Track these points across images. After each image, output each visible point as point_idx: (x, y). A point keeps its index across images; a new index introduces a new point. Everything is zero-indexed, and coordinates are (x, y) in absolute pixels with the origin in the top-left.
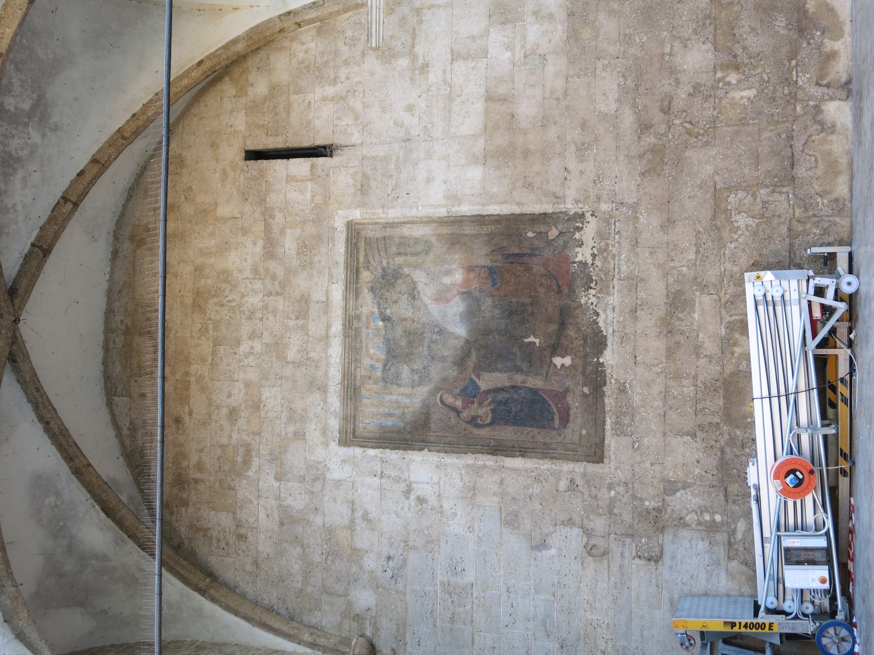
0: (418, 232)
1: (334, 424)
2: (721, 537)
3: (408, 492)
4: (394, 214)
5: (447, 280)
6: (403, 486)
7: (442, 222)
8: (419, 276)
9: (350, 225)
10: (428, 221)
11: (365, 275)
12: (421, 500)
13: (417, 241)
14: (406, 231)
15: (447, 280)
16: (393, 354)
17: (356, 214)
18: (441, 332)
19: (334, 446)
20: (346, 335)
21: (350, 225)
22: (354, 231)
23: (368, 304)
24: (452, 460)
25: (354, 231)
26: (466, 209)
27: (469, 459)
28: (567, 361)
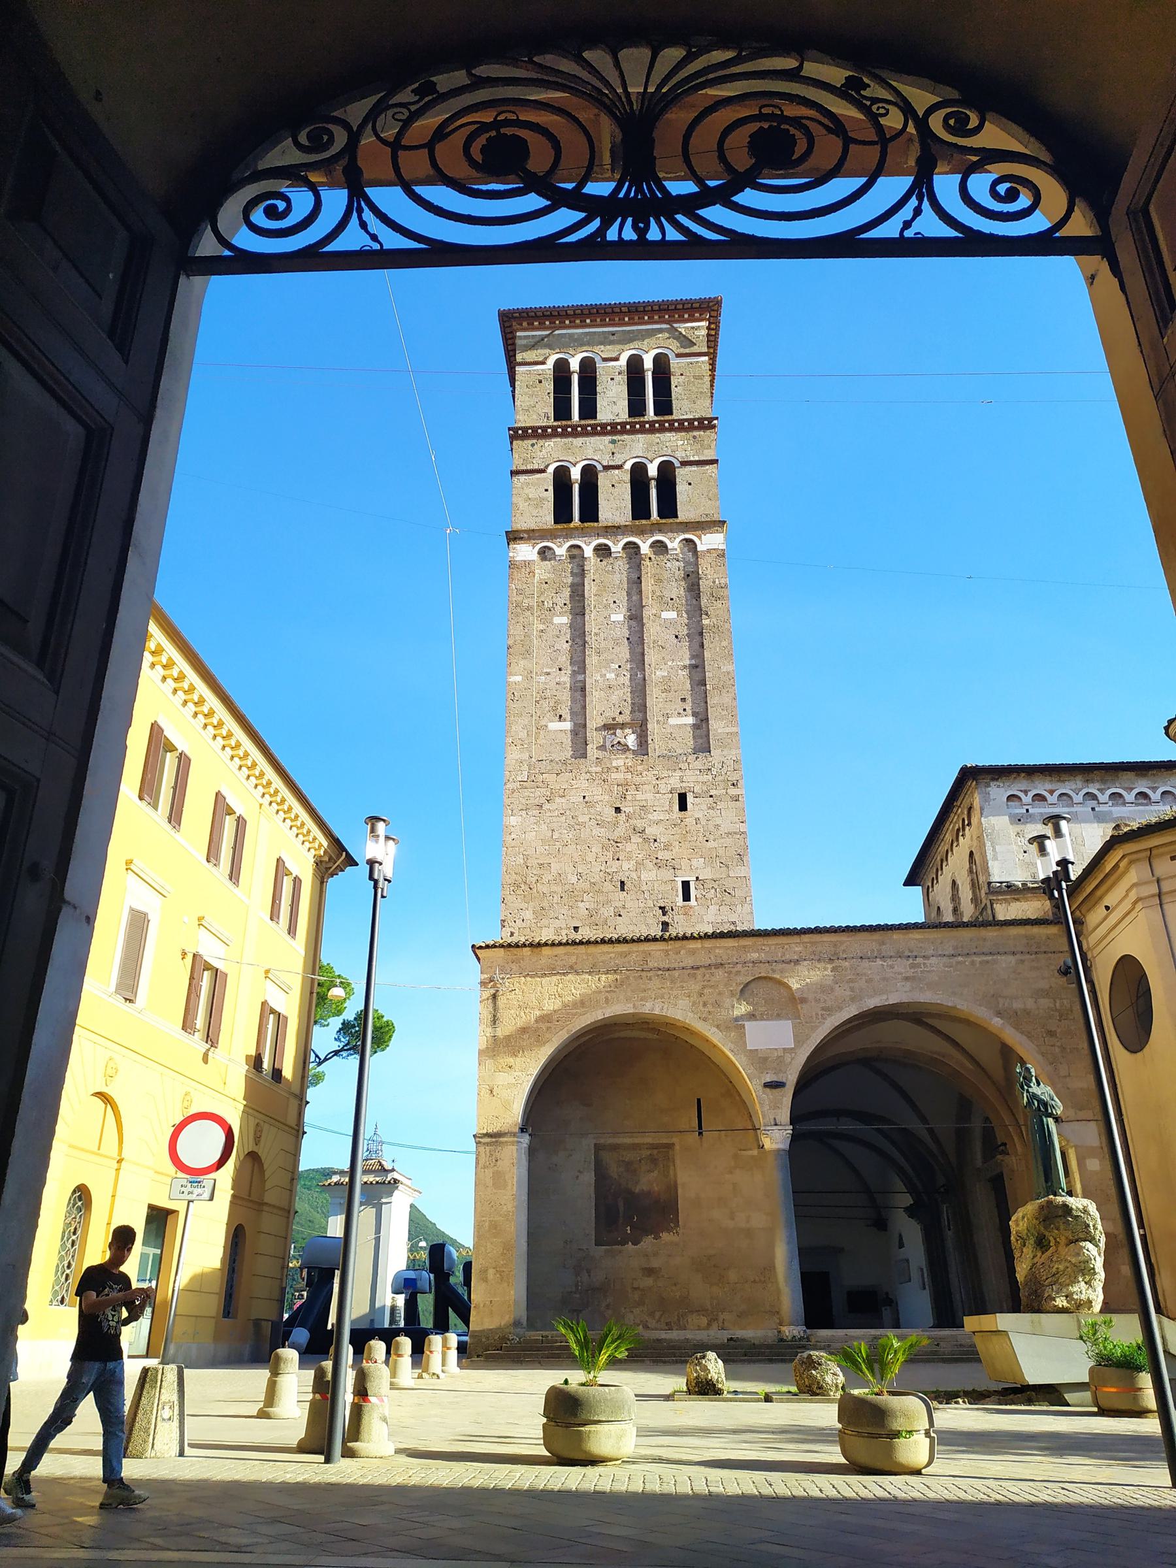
0: (671, 1172)
1: (602, 1141)
2: (574, 1289)
3: (579, 1171)
4: (678, 1162)
5: (655, 1185)
6: (582, 1170)
7: (676, 1182)
8: (655, 1173)
9: (673, 1144)
10: (675, 1175)
11: (655, 1152)
12: (578, 1177)
13: (668, 1172)
14: (672, 1167)
15: (655, 1185)
16: (628, 1165)
17: (677, 1147)
18: (637, 1183)
19: (595, 1141)
20: (634, 1144)
21: (673, 1144)
22: (670, 1146)
23: (647, 1153)
24: (592, 1189)
25: (670, 1146)
26: (680, 1191)
27: (593, 1196)
28: (629, 1232)
